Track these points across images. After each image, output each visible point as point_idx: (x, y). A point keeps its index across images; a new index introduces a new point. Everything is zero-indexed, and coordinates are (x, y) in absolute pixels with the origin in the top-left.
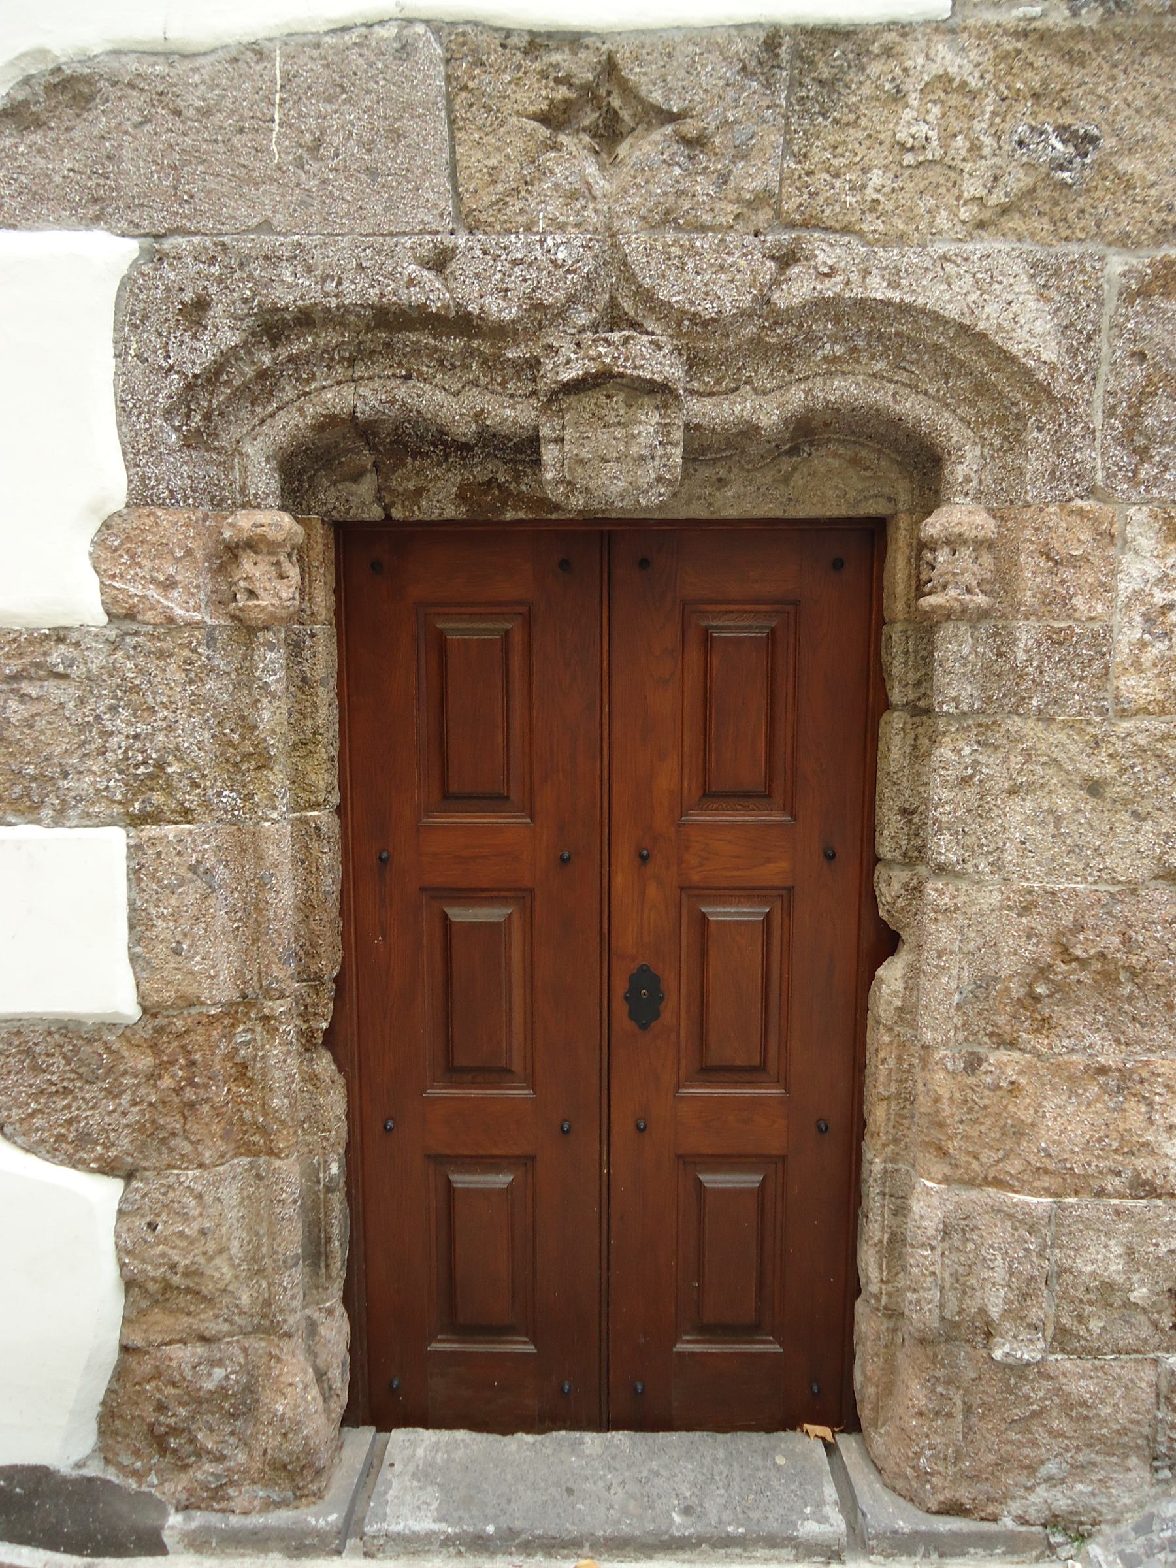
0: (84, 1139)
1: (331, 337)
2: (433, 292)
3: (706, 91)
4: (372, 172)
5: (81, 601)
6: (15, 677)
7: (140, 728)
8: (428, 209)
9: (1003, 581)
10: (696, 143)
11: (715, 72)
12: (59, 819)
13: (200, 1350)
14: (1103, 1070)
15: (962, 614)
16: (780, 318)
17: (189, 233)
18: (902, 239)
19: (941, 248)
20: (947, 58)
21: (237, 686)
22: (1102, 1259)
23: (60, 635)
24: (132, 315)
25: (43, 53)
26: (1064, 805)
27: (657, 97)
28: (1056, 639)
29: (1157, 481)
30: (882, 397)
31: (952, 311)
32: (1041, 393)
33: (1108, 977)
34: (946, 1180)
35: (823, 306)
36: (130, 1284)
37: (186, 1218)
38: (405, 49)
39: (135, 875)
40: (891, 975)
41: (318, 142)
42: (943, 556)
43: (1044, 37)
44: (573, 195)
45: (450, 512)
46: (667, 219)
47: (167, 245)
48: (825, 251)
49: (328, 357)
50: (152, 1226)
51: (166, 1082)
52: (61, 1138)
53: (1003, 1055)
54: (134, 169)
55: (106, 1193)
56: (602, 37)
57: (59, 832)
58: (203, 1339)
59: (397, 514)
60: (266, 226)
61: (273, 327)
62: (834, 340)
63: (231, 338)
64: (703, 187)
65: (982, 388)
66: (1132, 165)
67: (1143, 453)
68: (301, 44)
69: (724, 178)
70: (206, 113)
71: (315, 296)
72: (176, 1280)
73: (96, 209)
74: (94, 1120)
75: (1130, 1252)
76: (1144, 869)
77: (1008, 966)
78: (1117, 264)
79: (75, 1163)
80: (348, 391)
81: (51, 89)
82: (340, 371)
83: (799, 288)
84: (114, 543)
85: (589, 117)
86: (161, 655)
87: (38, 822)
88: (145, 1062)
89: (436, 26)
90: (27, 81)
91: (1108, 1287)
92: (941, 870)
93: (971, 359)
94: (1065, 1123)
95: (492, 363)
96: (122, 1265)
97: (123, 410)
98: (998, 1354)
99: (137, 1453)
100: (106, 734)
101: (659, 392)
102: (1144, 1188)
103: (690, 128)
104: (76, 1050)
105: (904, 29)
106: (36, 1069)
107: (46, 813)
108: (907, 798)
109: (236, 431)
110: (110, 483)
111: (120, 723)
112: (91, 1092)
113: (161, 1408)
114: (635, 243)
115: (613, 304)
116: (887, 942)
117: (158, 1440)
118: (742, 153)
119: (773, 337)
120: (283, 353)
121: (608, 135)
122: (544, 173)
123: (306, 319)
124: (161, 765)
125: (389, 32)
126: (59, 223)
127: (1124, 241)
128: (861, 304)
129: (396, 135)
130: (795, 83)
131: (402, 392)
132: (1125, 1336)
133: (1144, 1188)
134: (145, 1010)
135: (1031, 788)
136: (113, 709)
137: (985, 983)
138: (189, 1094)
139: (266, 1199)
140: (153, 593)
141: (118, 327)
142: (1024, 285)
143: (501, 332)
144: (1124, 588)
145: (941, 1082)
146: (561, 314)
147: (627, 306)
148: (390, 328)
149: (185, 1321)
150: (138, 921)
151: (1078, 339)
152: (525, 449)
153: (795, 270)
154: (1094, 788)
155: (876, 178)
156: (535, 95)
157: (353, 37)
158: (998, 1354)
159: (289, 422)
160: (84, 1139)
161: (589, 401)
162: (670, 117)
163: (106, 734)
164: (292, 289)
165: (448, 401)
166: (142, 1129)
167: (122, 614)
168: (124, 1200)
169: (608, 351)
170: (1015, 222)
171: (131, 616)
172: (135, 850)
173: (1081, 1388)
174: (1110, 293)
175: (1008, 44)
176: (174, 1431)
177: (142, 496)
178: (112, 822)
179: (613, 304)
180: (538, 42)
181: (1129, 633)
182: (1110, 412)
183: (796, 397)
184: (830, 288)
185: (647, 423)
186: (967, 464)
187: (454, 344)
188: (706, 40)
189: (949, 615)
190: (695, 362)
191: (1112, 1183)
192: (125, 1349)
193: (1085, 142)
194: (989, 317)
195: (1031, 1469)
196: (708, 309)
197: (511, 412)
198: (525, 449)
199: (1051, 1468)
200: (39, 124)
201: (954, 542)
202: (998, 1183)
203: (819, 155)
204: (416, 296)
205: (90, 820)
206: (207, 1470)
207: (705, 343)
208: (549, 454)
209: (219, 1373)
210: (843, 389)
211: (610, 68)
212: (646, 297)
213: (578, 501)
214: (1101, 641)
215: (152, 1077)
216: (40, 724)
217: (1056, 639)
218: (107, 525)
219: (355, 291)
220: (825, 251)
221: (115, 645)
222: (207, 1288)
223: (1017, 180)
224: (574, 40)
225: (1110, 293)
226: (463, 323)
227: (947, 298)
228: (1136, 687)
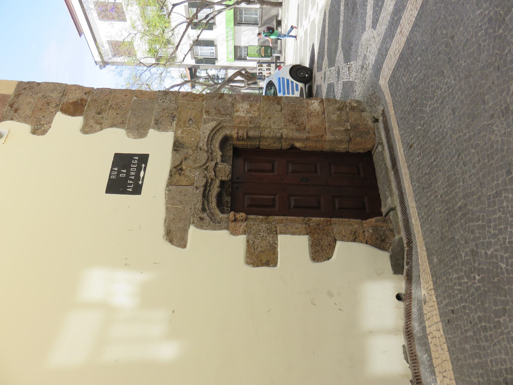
0: (330, 244)
1: (206, 203)
2: (202, 189)
3: (179, 157)
4: (185, 195)
5: (242, 239)
6: (254, 249)
7: (262, 231)
8: (190, 189)
9: (243, 128)
10: (186, 159)
11: (177, 156)
12: (277, 244)
13: (365, 233)
14: (308, 117)
15: (247, 132)
16: (208, 150)
17: (190, 219)
18: (200, 137)
19: (201, 133)
20: (179, 132)
21: (256, 221)
22: (334, 117)
23: (248, 241)
24: (201, 227)
25: (163, 236)
26: (272, 121)
27: (179, 162)
28: (250, 122)
29: (231, 113)
30: (218, 141)
31: (209, 132)
32: (219, 123)
33: (295, 117)
34: (326, 135)
35: (207, 145)
36: (354, 241)
37: (341, 231)
38: (169, 190)
39: (285, 233)
40: (298, 145)
41: (180, 201)
42: (239, 135)
43: (178, 123)
44: (191, 172)
45: (230, 198)
46: (195, 161)
47: (191, 222)
48: (201, 145)
49: (208, 205)
50: (344, 236)
51: (319, 232)
52: (330, 248)
53: (307, 128)
54: (181, 225)
55: (339, 244)
56: (171, 168)
57: (279, 244)
58: (364, 232)
59: (229, 205)
60: (191, 209)
61: (204, 210)
62: (211, 146)
63: (205, 215)
64: (191, 158)
65: (218, 130)
66: (194, 115)
67: (228, 114)
68: (167, 203)
69: (190, 155)
70: (174, 215)
71: (201, 203)
72: (353, 233)
73: (186, 231)
74: (326, 243)
75: (333, 114)
76: (280, 113)
77: (294, 127)
78: (205, 116)
79: (334, 247)
80: (213, 203)
81: (168, 236)
82: (210, 204)
83: (205, 148)
84: (234, 233)
85: (180, 171)
86: (251, 228)
87: (277, 248)
88: (316, 235)
89: (167, 186)
90: (167, 239)
91: (338, 116)
92: (282, 135)
93: (214, 131)
94: (315, 122)
95: (210, 185)
96: (351, 241)
97: (214, 230)
98: (350, 128)
99: (387, 244)
100: (263, 236)
101: (216, 164)
102: (323, 113)
103: (183, 159)
104: (315, 245)
105: (175, 136)
106: (318, 251)
107: (276, 246)
108: (272, 142)
109: (218, 219)
110: (225, 233)
111: (262, 234)
112: (322, 243)
113: (377, 239)
114: (198, 165)
115: (205, 169)
116: (293, 147)
117: (383, 241)
118: (187, 153)
119: (210, 152)
120: (207, 209)
121: (181, 169)
122: (187, 175)
123: (203, 204)
124: (268, 229)
125: (167, 192)
126: (187, 236)
127: (202, 115)
128: (207, 141)
129: (180, 192)
130: (180, 147)
131: (214, 196)
132: (345, 115)
133: (323, 113)
134: (307, 235)
135: (270, 125)
136: (259, 235)
137: (297, 130)
138: (321, 229)
139: (339, 225)
140: (242, 227)
141: (202, 229)
142: (207, 125)
143: (207, 182)
144: (244, 115)
145: (312, 135)
146: (205, 175)
147: (205, 167)
148: (205, 196)
149: (361, 234)
150: (293, 234)
151: (213, 120)
152: (222, 183)
153: (202, 148)
154: (270, 118)
155: (192, 139)
156: (177, 176)
157: (167, 196)
158: (350, 128)
159: (217, 211)
160: (330, 244)
161: (217, 173)
162: (182, 161)
163: (263, 236)
164: (199, 206)
165: (215, 190)
166: (327, 236)
167: (244, 233)
168: (340, 240)
169: (211, 169)
170: (199, 126)
171: (245, 232)
172: (281, 233)
173: (353, 119)
174: (208, 117)
175: (178, 126)
176: (381, 237)
177: (227, 228)
178: (277, 237)
179: (205, 169)
180: (171, 175)
181: (250, 115)
182: (223, 117)
183: (218, 150)
184: (205, 144)
185: (219, 166)
186: (228, 132)
187: (208, 188)
188: (173, 157)
189: (247, 135)
190: (212, 160)
191: (323, 116)
192: (367, 243)
193: (190, 119)
194: (210, 128)
195: (366, 125)
196: (207, 157)
197: (217, 183)
198: (222, 183)
199: (366, 122)
200: (172, 239)
201: (238, 133)
202: (325, 129)
203: (189, 145)
204: (202, 191)
205: (277, 240)
206: (387, 233)
207: (211, 158)
208: (224, 178)
209: (370, 231)
210: (217, 145)
211: (175, 167)
212: (204, 164)
213: (230, 176)
214: (251, 118)
215: (318, 233)
216: (262, 245)
217: (250, 122)
218: (231, 234)
219: (200, 198)
220: (201, 145)
221: (249, 234)
222: (355, 230)
223: (194, 126)
224: (171, 171)
225: (208, 117)
226: (205, 186)
227: (207, 133)
228: (257, 114)
